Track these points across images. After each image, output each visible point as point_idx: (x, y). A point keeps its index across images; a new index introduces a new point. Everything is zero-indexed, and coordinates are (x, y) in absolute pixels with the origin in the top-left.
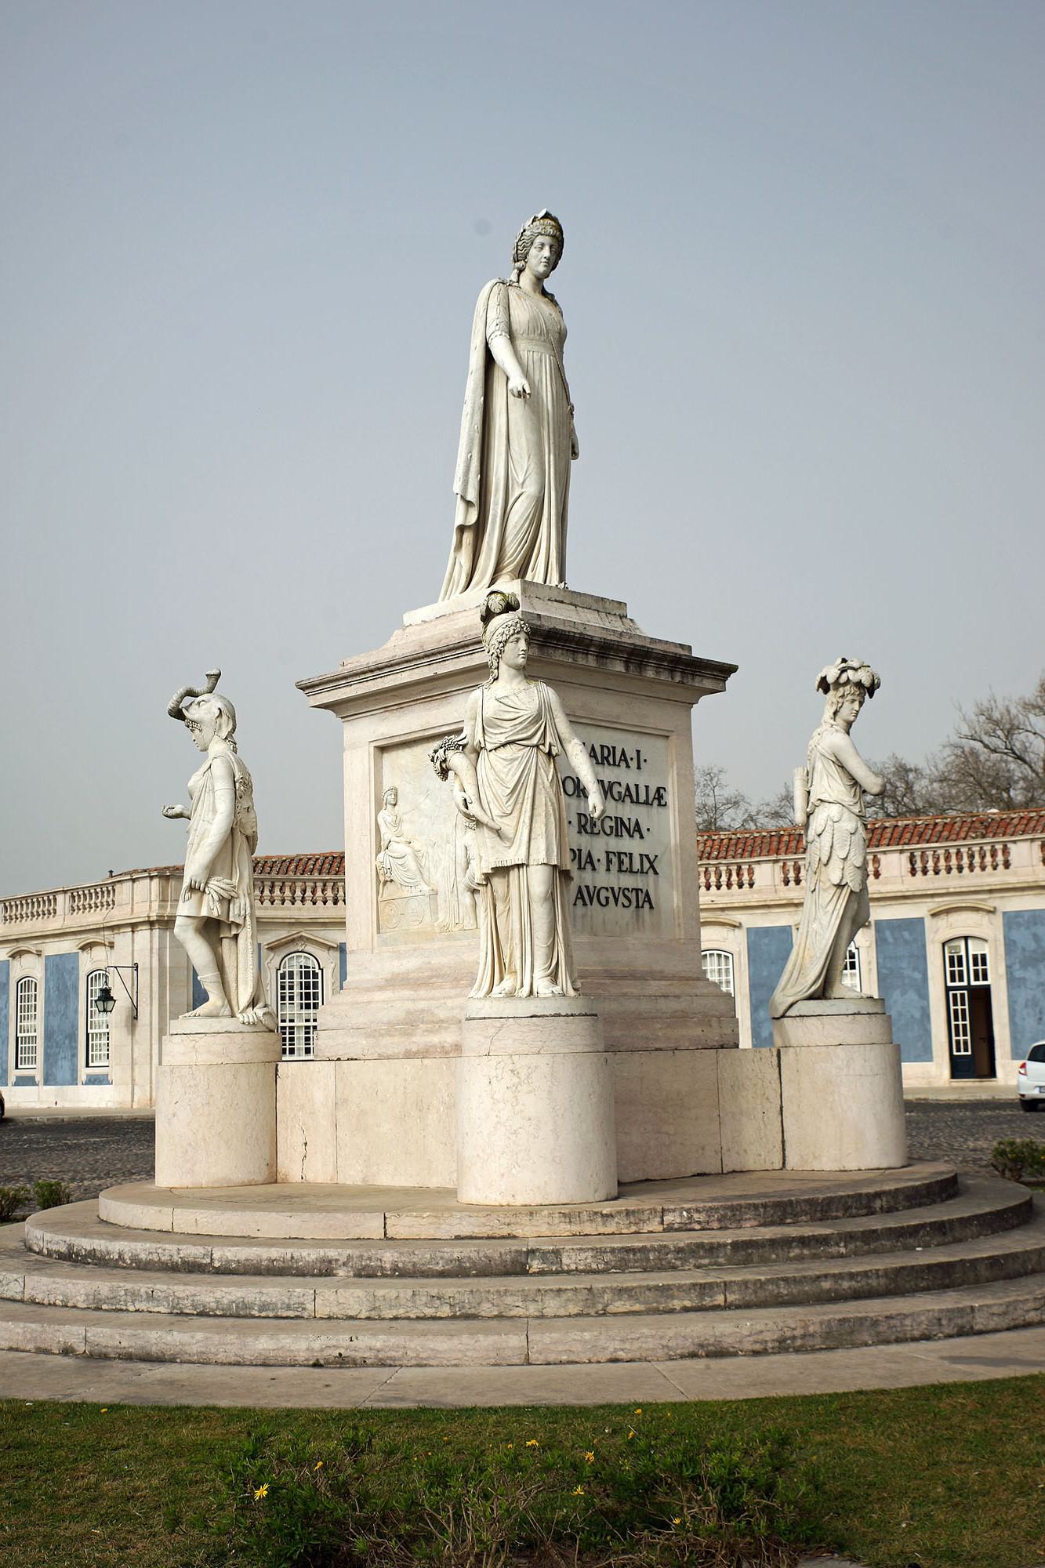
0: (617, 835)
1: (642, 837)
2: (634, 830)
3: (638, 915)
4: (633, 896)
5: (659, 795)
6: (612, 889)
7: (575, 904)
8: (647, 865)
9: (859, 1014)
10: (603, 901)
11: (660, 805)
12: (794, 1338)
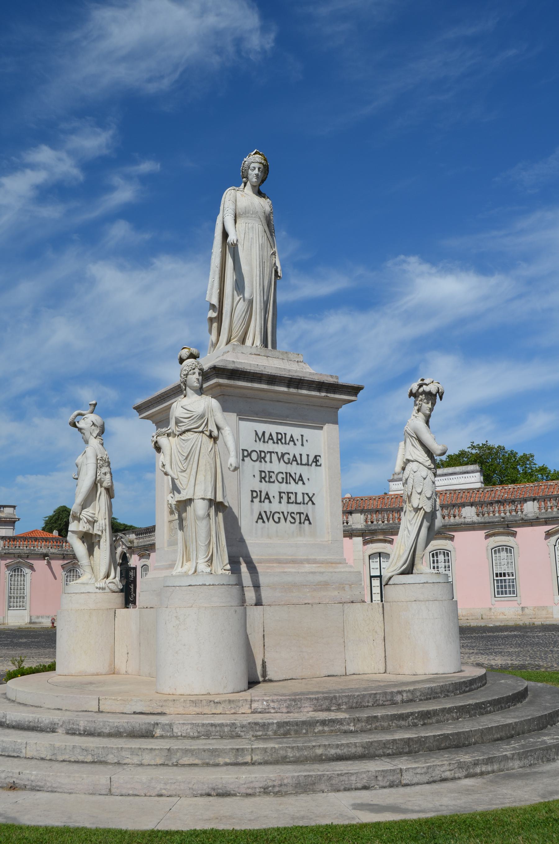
0: (287, 483)
1: (304, 484)
2: (299, 480)
3: (300, 527)
4: (297, 517)
5: (316, 460)
6: (283, 513)
7: (257, 522)
9: (427, 583)
10: (277, 520)
11: (316, 465)
12: (274, 786)
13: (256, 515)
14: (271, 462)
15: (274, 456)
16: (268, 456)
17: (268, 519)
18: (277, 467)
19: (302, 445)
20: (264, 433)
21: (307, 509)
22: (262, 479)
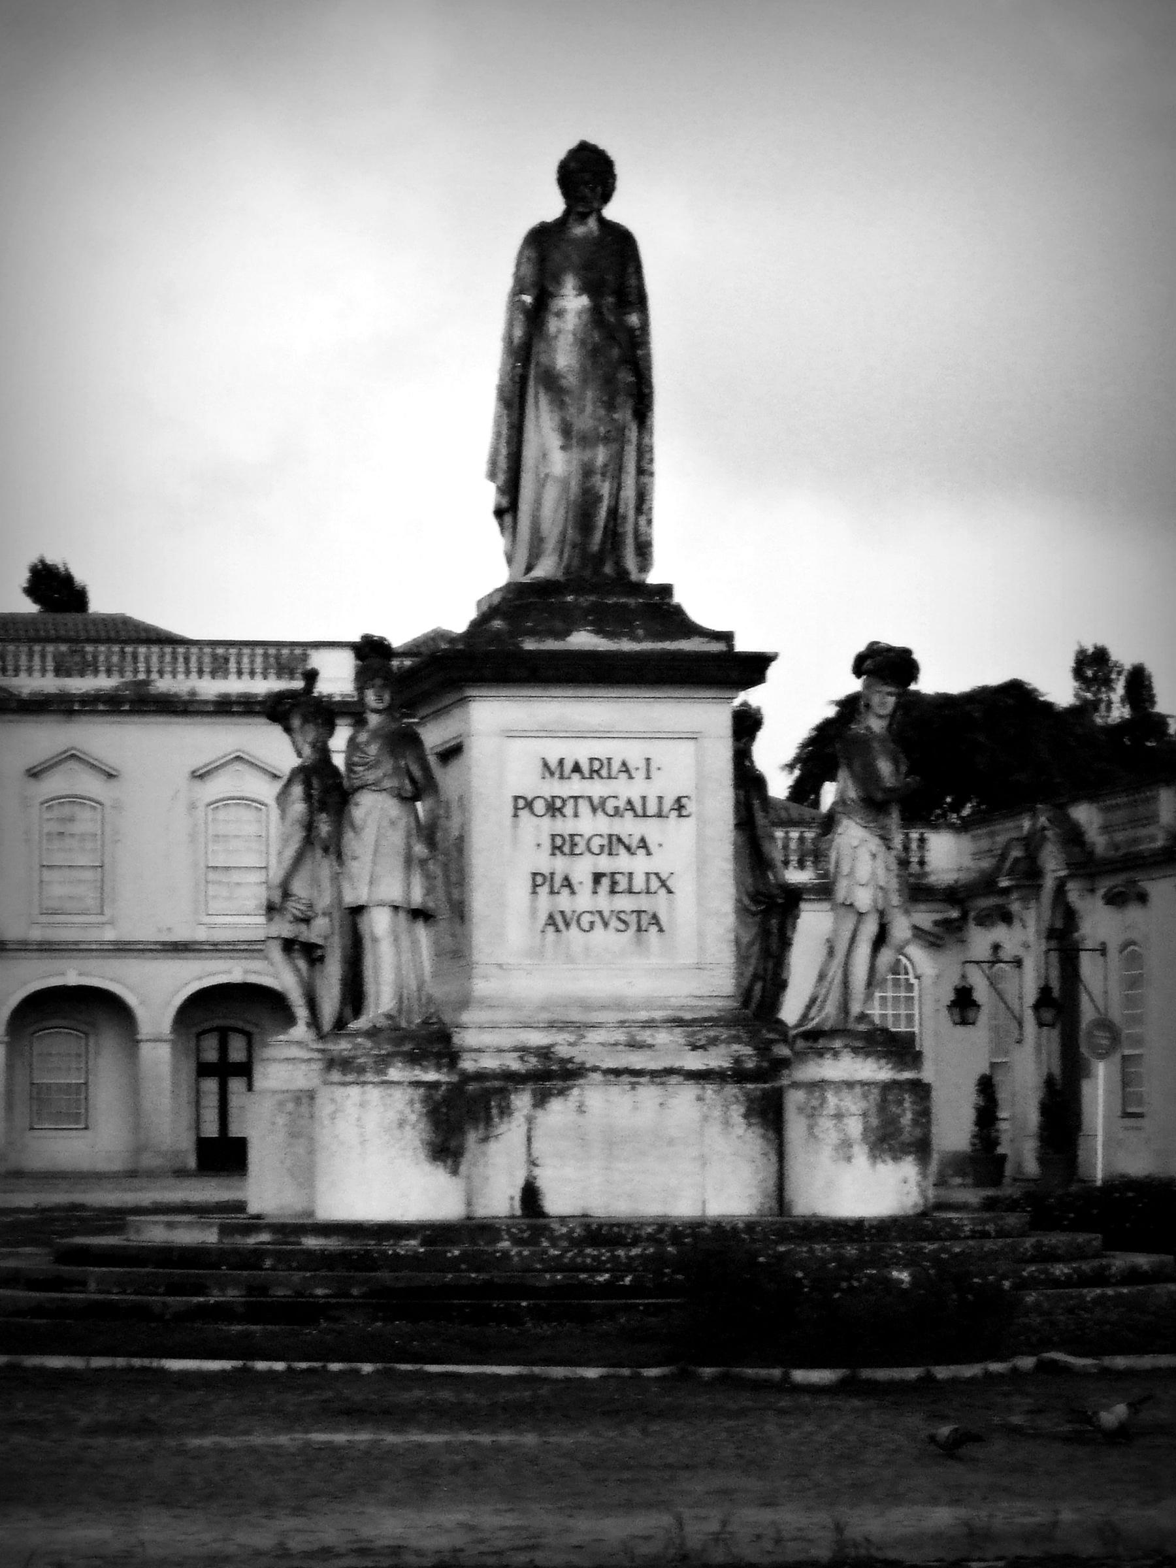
1: (649, 854)
3: (639, 942)
4: (632, 919)
5: (679, 806)
8: (655, 884)
13: (543, 917)
14: (576, 815)
15: (584, 807)
16: (571, 803)
17: (567, 925)
18: (588, 825)
19: (648, 778)
20: (561, 762)
21: (659, 903)
22: (556, 849)
